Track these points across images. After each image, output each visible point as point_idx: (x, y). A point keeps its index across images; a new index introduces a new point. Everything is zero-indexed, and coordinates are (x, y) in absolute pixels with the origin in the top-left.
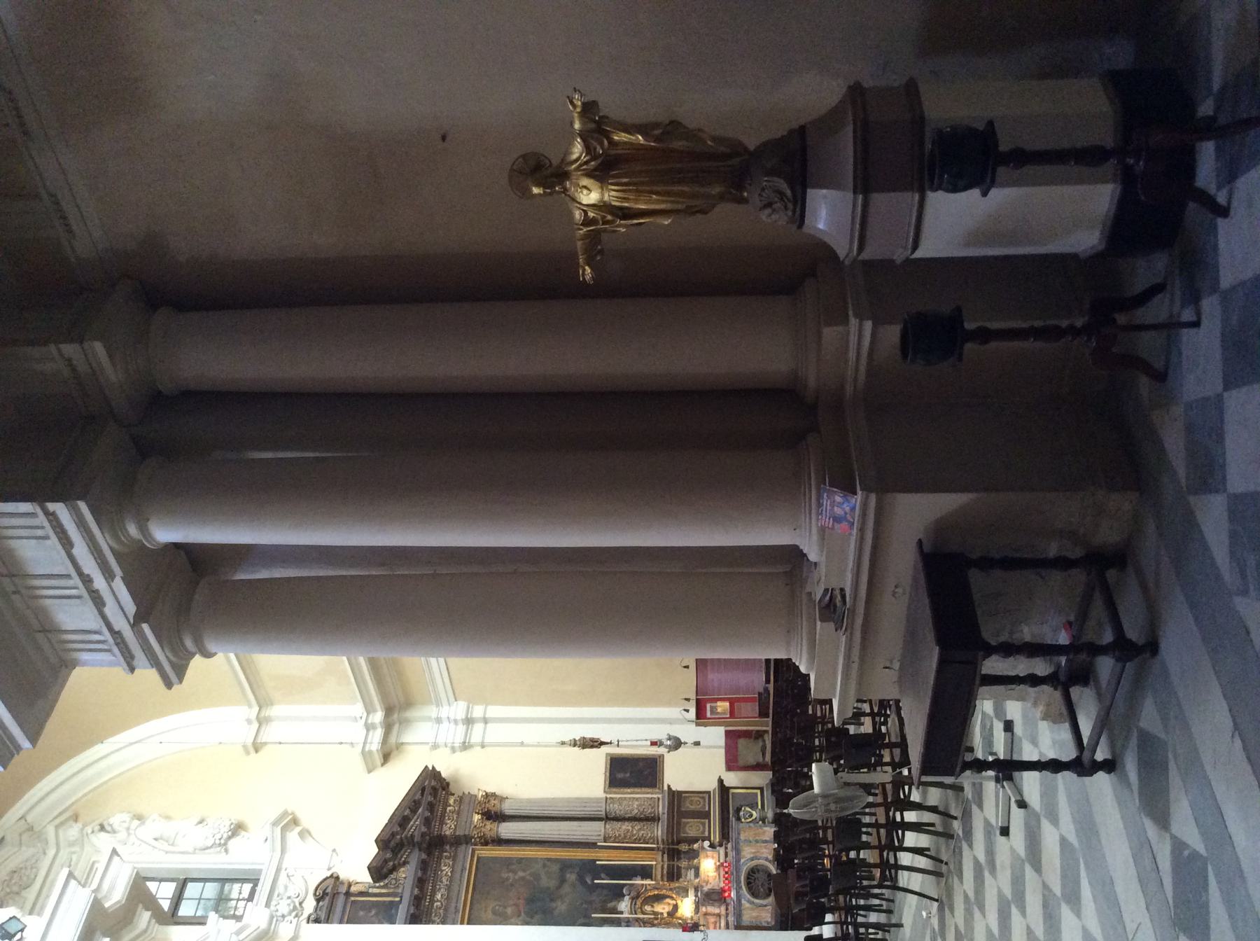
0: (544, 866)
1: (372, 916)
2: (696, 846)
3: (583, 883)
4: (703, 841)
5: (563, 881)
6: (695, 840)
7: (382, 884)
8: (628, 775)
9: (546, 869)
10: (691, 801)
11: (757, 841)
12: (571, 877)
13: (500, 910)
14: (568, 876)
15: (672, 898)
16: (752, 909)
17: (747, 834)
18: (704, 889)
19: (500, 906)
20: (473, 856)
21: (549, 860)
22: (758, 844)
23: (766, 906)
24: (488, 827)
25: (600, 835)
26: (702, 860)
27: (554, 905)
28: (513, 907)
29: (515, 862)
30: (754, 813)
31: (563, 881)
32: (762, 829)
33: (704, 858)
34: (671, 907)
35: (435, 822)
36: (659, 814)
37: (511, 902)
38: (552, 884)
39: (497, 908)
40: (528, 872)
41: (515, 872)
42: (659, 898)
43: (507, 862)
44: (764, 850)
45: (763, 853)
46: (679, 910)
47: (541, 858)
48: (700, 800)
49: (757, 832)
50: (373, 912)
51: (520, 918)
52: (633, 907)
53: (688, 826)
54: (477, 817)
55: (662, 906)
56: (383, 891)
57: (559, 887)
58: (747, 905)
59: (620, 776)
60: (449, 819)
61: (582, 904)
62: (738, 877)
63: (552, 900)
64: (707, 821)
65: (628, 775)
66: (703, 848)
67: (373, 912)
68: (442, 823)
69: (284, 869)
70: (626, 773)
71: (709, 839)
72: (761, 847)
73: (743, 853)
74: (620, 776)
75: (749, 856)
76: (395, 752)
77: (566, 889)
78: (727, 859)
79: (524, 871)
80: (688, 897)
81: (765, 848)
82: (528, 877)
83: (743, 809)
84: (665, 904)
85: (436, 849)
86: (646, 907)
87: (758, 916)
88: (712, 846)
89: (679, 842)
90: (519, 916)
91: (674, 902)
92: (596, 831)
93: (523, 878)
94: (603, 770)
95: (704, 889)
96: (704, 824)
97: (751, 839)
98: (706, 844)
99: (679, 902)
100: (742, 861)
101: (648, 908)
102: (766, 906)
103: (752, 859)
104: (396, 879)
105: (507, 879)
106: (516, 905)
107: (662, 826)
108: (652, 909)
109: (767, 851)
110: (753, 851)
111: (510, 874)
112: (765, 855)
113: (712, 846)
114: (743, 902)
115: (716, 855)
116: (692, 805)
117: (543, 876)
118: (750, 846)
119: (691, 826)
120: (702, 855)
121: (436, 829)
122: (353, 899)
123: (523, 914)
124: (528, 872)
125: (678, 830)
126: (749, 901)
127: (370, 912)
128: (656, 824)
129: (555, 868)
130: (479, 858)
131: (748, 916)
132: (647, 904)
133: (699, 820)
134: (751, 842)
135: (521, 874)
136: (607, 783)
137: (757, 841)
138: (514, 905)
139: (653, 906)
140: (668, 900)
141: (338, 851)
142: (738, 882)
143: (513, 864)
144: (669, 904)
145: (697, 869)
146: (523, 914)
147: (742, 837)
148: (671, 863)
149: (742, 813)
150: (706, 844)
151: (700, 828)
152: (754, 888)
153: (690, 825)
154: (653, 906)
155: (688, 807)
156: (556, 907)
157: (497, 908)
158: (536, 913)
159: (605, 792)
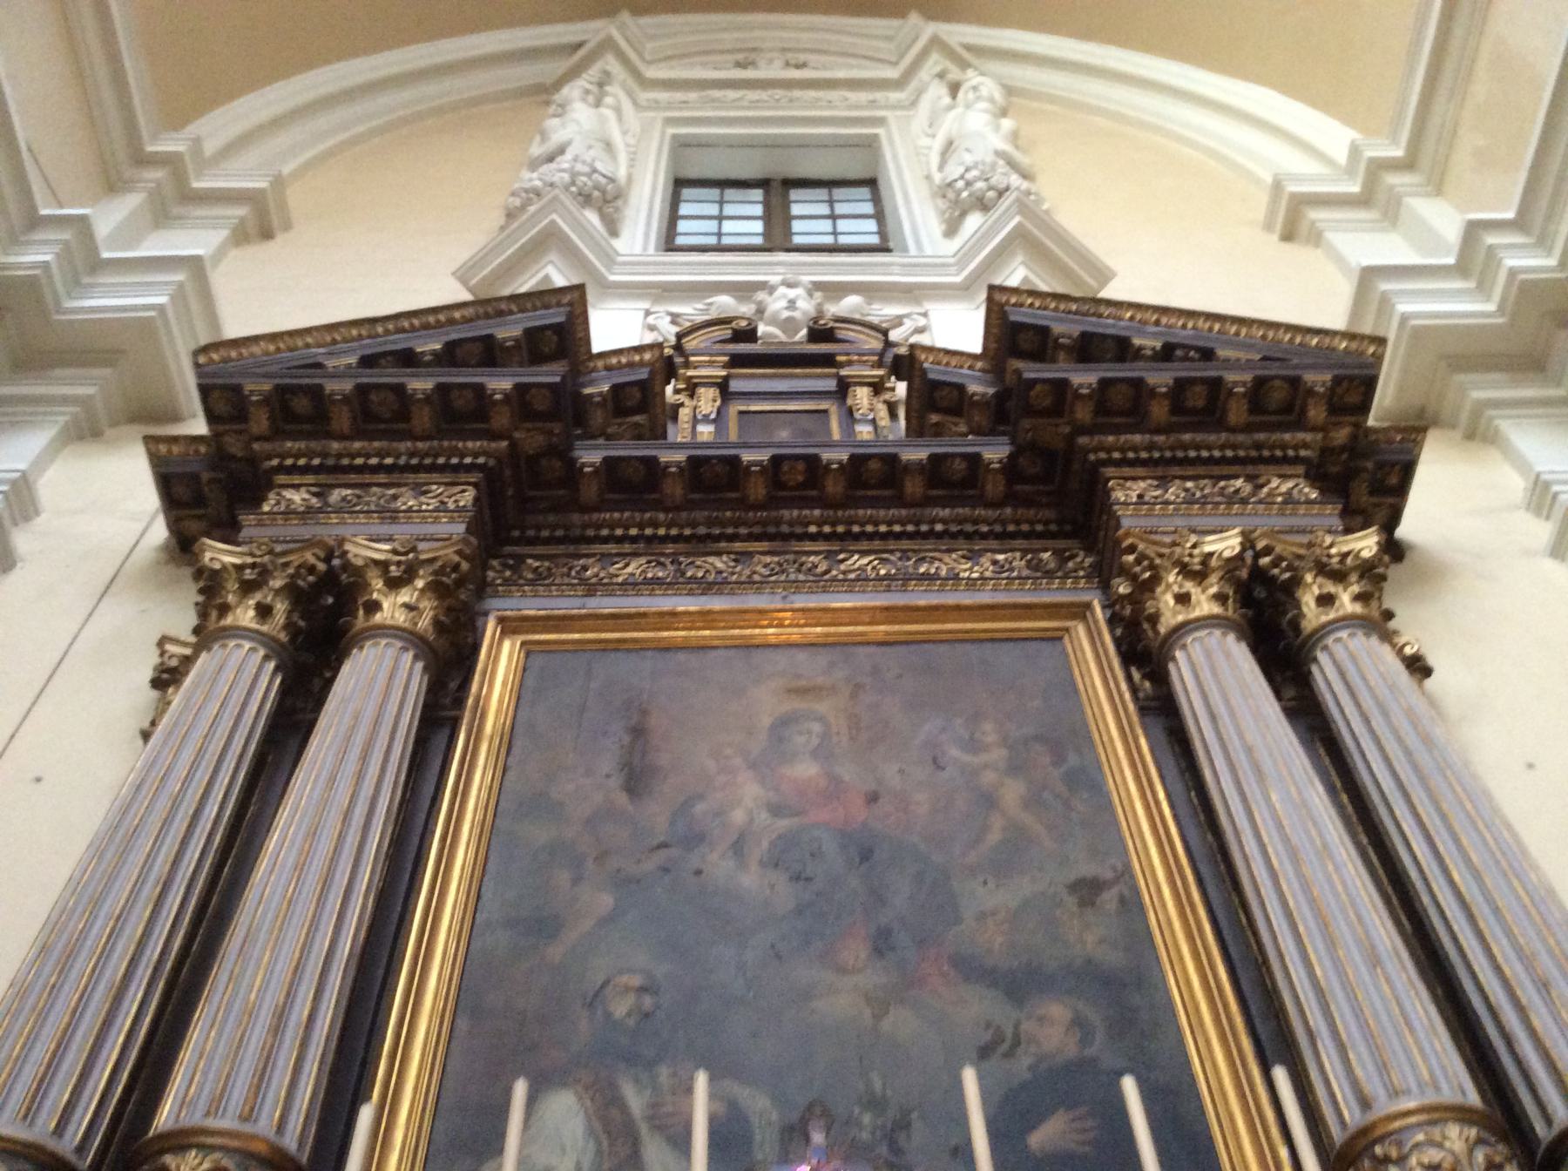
0: (1087, 891)
9: (1071, 901)
13: (800, 740)
14: (1058, 1011)
19: (825, 736)
21: (1132, 905)
25: (1365, 1103)
27: (856, 951)
29: (1073, 760)
37: (847, 772)
38: (993, 942)
39: (817, 727)
40: (1028, 819)
41: (1015, 768)
47: (1128, 867)
51: (763, 817)
57: (971, 969)
61: (875, 1103)
63: (882, 944)
69: (922, 311)
79: (1033, 802)
82: (997, 822)
90: (776, 810)
92: (1383, 1068)
93: (989, 801)
111: (998, 755)
117: (1024, 887)
123: (783, 824)
124: (1028, 819)
138: (836, 781)
143: (1059, 759)
146: (783, 824)
156: (842, 970)
157: (817, 727)
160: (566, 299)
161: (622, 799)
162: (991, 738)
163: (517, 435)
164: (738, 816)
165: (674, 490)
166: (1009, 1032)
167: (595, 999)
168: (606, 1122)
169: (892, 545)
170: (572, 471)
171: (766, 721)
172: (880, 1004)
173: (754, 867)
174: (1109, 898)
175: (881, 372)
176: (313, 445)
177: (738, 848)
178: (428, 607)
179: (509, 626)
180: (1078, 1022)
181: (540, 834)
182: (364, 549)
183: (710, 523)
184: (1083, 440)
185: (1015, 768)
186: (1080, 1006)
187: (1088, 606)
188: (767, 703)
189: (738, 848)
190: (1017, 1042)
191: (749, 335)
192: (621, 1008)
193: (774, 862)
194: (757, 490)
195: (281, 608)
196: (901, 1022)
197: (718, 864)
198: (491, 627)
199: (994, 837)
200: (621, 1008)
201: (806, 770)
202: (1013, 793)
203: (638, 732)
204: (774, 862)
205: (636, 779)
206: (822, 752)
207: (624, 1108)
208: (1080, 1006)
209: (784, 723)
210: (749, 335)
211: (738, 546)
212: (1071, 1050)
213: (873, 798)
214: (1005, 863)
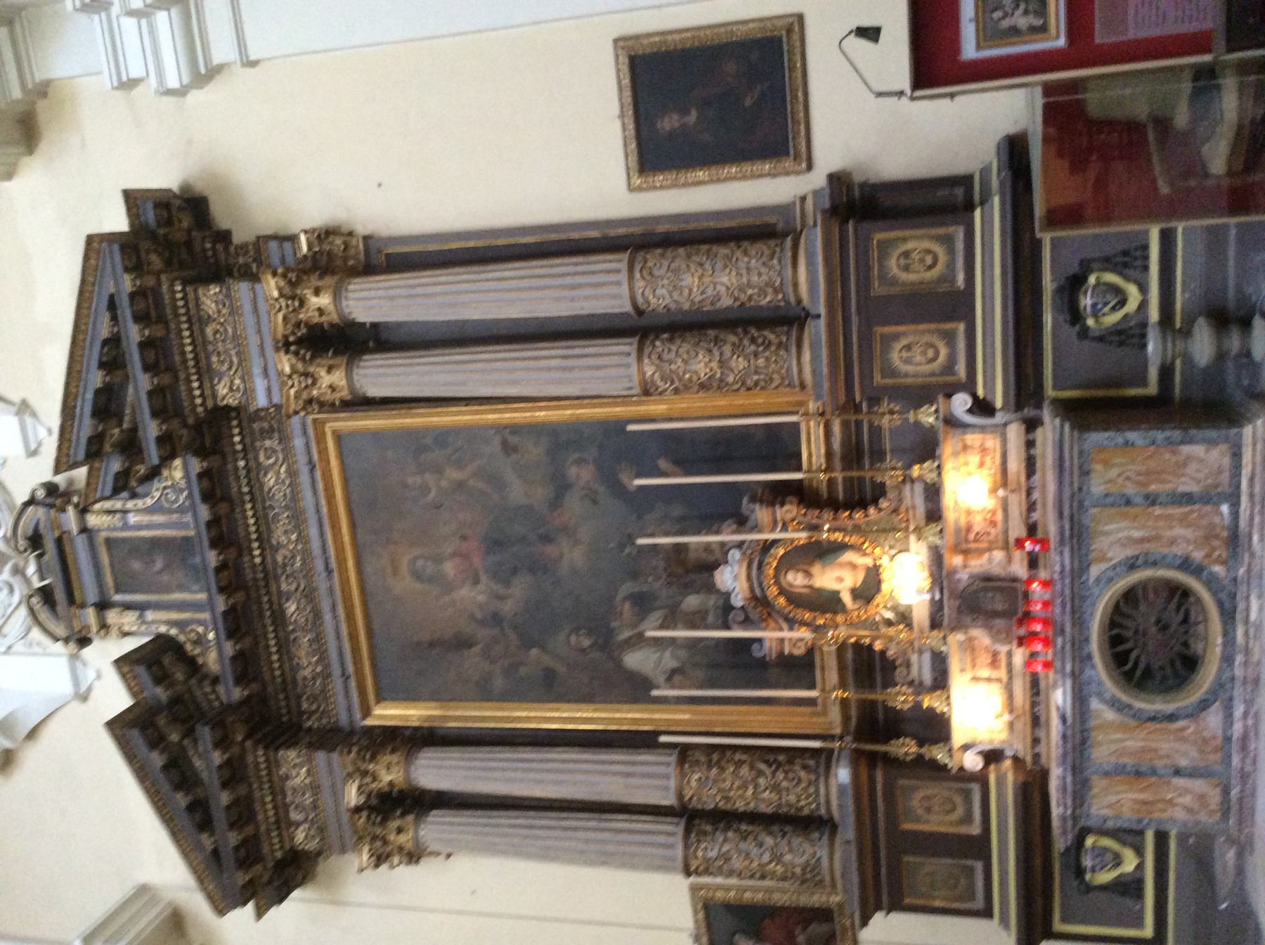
0: (508, 448)
1: (159, 572)
2: (927, 416)
3: (619, 491)
4: (949, 396)
5: (562, 487)
6: (922, 394)
7: (149, 502)
8: (693, 117)
9: (514, 457)
10: (906, 254)
11: (1152, 500)
12: (582, 474)
14: (573, 471)
15: (857, 548)
16: (1123, 728)
17: (1113, 473)
18: (958, 576)
19: (426, 559)
20: (321, 438)
21: (515, 429)
22: (1158, 511)
23: (1172, 718)
24: (326, 379)
26: (949, 466)
27: (551, 550)
28: (457, 560)
29: (429, 441)
30: (1132, 290)
31: (562, 487)
32: (1174, 453)
33: (955, 454)
34: (860, 577)
35: (189, 382)
36: (799, 301)
37: (449, 549)
38: (540, 494)
40: (470, 469)
41: (438, 470)
42: (823, 552)
43: (417, 442)
44: (1179, 531)
45: (1173, 542)
46: (885, 587)
48: (940, 250)
49: (1152, 464)
50: (159, 564)
51: (481, 587)
52: (754, 572)
53: (898, 346)
54: (285, 363)
55: (837, 573)
56: (158, 518)
57: (556, 503)
58: (1110, 715)
59: (669, 123)
60: (222, 362)
62: (1080, 622)
63: (547, 539)
64: (961, 327)
65: (693, 117)
66: (951, 422)
67: (159, 564)
68: (206, 373)
70: (685, 112)
71: (969, 386)
72: (1168, 517)
73: (1100, 544)
74: (669, 123)
75: (1119, 554)
76: (41, 105)
77: (574, 504)
78: (1037, 478)
79: (459, 464)
80: (907, 550)
81: (1183, 520)
82: (471, 482)
83: (1092, 280)
84: (841, 565)
85: (230, 419)
86: (791, 577)
87: (1143, 750)
88: (983, 407)
89: (874, 401)
90: (476, 581)
91: (868, 561)
93: (460, 486)
94: (615, 108)
95: (958, 576)
96: (950, 338)
97: (1130, 490)
98: (961, 403)
99: (885, 561)
100: (1095, 571)
101: (795, 579)
102: (1172, 718)
103: (1132, 565)
104: (172, 486)
105: (425, 490)
106: (463, 556)
107: (814, 347)
108: (806, 582)
109: (1188, 533)
110: (1137, 534)
112: (1179, 550)
113: (983, 407)
114: (1095, 704)
115: (992, 442)
116: (906, 268)
117: (510, 476)
118: (1125, 516)
119: (908, 347)
120: (948, 448)
121: (199, 401)
122: (104, 534)
124: (470, 469)
125: (867, 375)
126: (1114, 704)
127: (154, 562)
128: (794, 334)
129: (535, 451)
130: (338, 437)
131: (1113, 747)
132: (792, 567)
133: (933, 326)
134: (1128, 502)
135: (453, 474)
136: (633, 158)
137: (1152, 500)
138: (455, 554)
139: (808, 574)
140: (849, 556)
141: (33, 401)
142: (1079, 643)
144: (853, 566)
145: (933, 492)
146: (484, 578)
147: (1097, 487)
148: (855, 474)
149: (1086, 301)
150: (961, 403)
151: (937, 353)
152: (1133, 656)
153: (904, 342)
154: (808, 574)
155: (894, 282)
156: (562, 556)
157: (420, 563)
158: (515, 571)
159: (631, 189)
160: (119, 732)
161: (476, 650)
162: (418, 480)
163: (239, 738)
164: (481, 598)
165: (248, 641)
166: (583, 493)
167: (583, 651)
168: (634, 645)
169: (260, 513)
170: (245, 702)
171: (418, 586)
172: (576, 543)
173: (510, 591)
174: (513, 440)
175: (70, 509)
176: (264, 838)
177: (501, 598)
178: (387, 758)
179: (367, 713)
180: (579, 462)
181: (499, 683)
182: (352, 795)
183: (261, 616)
184: (191, 421)
185: (438, 470)
186: (568, 463)
187: (315, 421)
188: (404, 584)
189: (501, 598)
190: (590, 489)
191: (46, 594)
192: (586, 642)
193: (507, 583)
194: (240, 596)
195: (394, 824)
196: (584, 533)
197: (508, 607)
198: (369, 722)
199: (481, 485)
200: (586, 642)
201: (449, 568)
202: (453, 474)
203: (432, 644)
204: (507, 583)
205: (462, 643)
206: (438, 559)
207: (630, 638)
208: (571, 459)
209: (418, 576)
210: (46, 594)
211: (275, 598)
212: (591, 467)
213: (464, 538)
214: (497, 482)
